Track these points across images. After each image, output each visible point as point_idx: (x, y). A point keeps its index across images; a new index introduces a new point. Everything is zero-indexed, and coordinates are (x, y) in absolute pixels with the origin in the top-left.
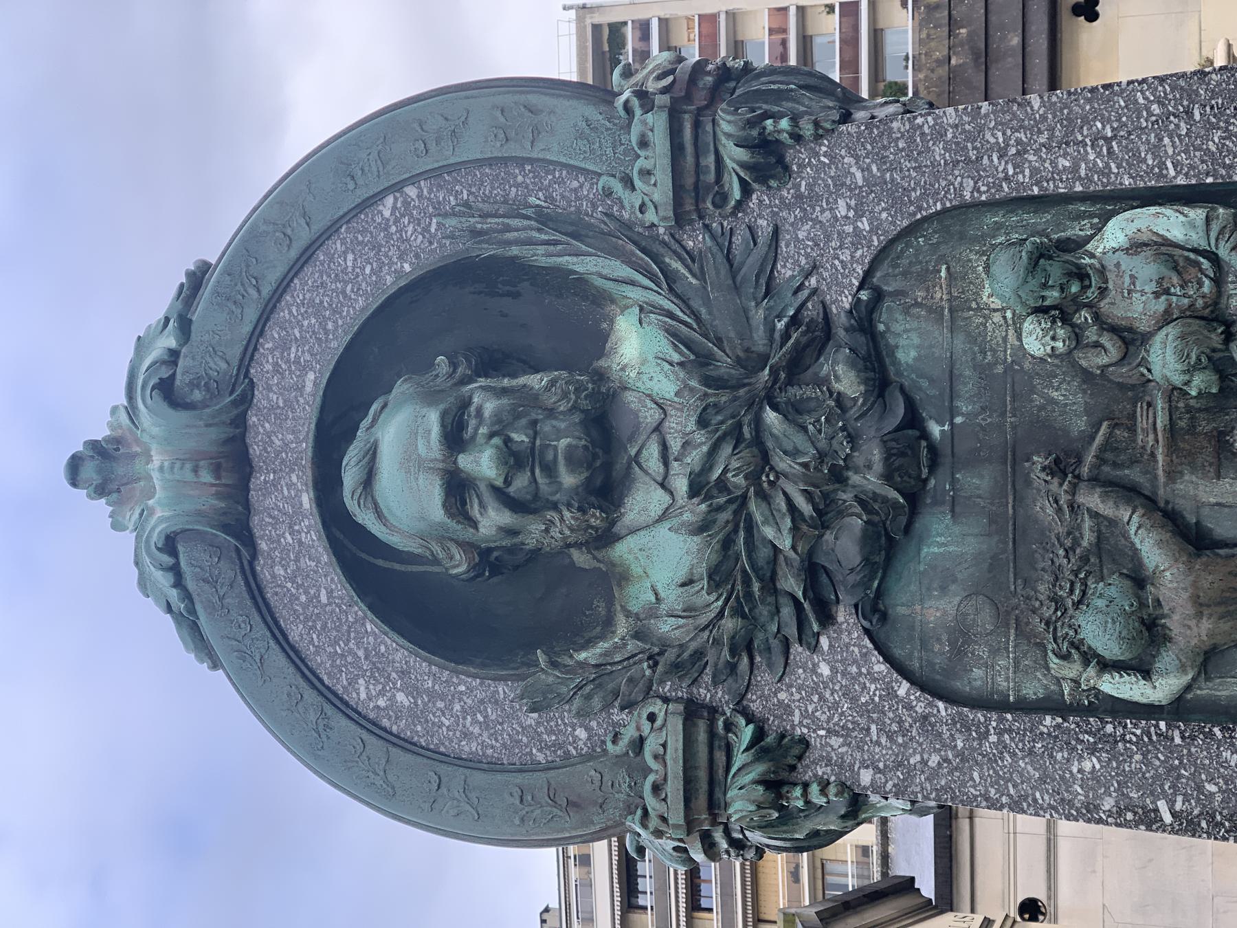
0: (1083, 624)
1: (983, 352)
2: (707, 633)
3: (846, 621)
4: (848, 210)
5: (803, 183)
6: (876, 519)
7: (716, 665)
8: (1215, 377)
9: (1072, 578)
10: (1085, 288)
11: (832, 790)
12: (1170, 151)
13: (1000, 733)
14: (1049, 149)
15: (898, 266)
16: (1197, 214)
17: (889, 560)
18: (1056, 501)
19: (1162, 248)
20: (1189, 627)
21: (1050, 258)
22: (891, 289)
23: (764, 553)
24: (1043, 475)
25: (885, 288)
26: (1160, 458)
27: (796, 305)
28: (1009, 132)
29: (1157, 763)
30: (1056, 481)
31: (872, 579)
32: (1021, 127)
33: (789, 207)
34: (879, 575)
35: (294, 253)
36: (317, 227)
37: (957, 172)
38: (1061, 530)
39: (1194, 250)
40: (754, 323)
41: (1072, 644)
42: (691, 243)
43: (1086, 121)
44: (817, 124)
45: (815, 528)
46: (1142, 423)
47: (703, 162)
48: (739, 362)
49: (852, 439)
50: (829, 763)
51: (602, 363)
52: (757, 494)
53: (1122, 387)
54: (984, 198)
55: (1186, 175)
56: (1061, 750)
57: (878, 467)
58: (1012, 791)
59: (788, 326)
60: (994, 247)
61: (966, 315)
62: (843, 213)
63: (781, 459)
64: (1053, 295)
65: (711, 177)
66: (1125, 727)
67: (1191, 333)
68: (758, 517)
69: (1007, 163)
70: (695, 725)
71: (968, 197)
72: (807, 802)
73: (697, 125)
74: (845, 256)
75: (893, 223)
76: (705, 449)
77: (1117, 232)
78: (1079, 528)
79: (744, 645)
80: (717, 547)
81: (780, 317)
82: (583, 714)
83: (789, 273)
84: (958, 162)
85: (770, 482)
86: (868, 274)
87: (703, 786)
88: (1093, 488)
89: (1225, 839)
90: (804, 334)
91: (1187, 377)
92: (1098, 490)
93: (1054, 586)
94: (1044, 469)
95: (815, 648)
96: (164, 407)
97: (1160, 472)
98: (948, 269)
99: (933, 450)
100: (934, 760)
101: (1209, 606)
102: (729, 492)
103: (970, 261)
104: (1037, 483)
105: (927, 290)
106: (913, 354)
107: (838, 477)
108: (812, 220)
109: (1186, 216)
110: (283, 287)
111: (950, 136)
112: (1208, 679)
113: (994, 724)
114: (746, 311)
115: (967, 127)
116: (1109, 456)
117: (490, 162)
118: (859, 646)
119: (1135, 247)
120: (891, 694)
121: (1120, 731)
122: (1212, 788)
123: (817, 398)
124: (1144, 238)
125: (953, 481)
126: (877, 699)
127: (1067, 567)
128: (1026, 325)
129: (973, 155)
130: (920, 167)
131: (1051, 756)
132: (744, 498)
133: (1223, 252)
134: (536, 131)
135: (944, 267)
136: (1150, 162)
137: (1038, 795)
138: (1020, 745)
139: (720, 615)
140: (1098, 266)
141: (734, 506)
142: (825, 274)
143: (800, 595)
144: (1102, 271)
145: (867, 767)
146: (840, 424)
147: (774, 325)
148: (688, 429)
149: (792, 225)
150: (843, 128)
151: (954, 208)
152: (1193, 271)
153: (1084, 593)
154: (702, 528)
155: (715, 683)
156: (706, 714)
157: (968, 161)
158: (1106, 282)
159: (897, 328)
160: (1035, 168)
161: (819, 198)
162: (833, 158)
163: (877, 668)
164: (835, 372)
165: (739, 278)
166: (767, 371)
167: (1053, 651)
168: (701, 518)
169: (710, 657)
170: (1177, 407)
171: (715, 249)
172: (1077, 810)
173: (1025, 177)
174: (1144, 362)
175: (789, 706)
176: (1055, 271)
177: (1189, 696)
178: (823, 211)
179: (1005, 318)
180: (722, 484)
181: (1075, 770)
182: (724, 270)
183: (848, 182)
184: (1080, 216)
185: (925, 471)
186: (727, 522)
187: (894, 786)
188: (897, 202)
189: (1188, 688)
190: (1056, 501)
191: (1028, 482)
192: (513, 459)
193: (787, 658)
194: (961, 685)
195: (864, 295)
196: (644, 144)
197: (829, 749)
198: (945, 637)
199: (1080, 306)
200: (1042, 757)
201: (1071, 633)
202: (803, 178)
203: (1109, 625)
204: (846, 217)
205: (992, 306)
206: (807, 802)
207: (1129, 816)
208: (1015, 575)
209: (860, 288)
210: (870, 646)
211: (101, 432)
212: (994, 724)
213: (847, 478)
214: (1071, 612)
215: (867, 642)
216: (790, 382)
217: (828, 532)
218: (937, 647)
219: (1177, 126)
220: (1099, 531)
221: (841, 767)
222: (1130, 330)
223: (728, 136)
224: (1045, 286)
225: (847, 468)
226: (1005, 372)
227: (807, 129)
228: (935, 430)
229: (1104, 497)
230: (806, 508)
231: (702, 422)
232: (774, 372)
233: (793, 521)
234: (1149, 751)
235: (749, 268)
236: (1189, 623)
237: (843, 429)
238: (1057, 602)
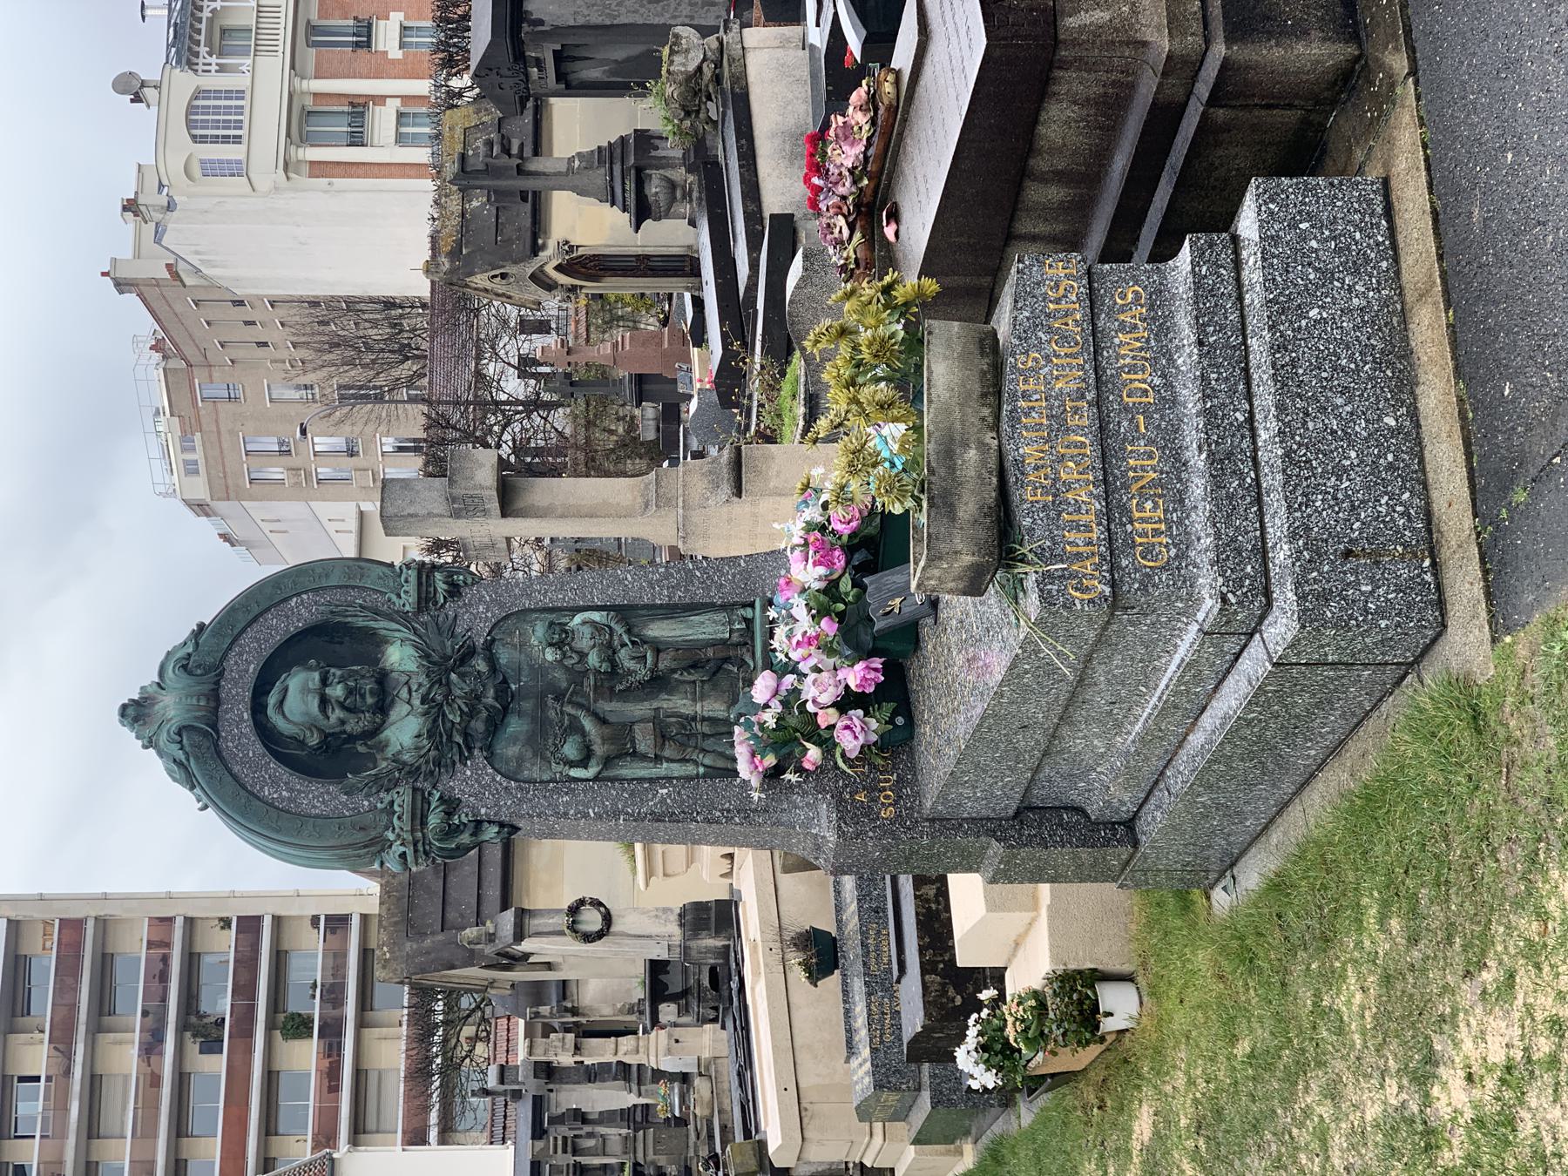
16: (605, 613)
17: (494, 733)
19: (593, 623)
35: (250, 618)
36: (261, 609)
51: (380, 665)
73: (428, 576)
77: (578, 619)
79: (438, 764)
82: (368, 796)
96: (185, 675)
107: (478, 698)
110: (244, 630)
117: (340, 587)
119: (584, 623)
120: (494, 780)
132: (442, 705)
134: (362, 576)
144: (573, 631)
154: (425, 714)
155: (425, 780)
173: (547, 601)
180: (433, 700)
188: (501, 606)
189: (599, 773)
192: (350, 692)
196: (406, 581)
211: (136, 697)
216: (460, 666)
228: (513, 687)
230: (466, 710)
238: (556, 745)
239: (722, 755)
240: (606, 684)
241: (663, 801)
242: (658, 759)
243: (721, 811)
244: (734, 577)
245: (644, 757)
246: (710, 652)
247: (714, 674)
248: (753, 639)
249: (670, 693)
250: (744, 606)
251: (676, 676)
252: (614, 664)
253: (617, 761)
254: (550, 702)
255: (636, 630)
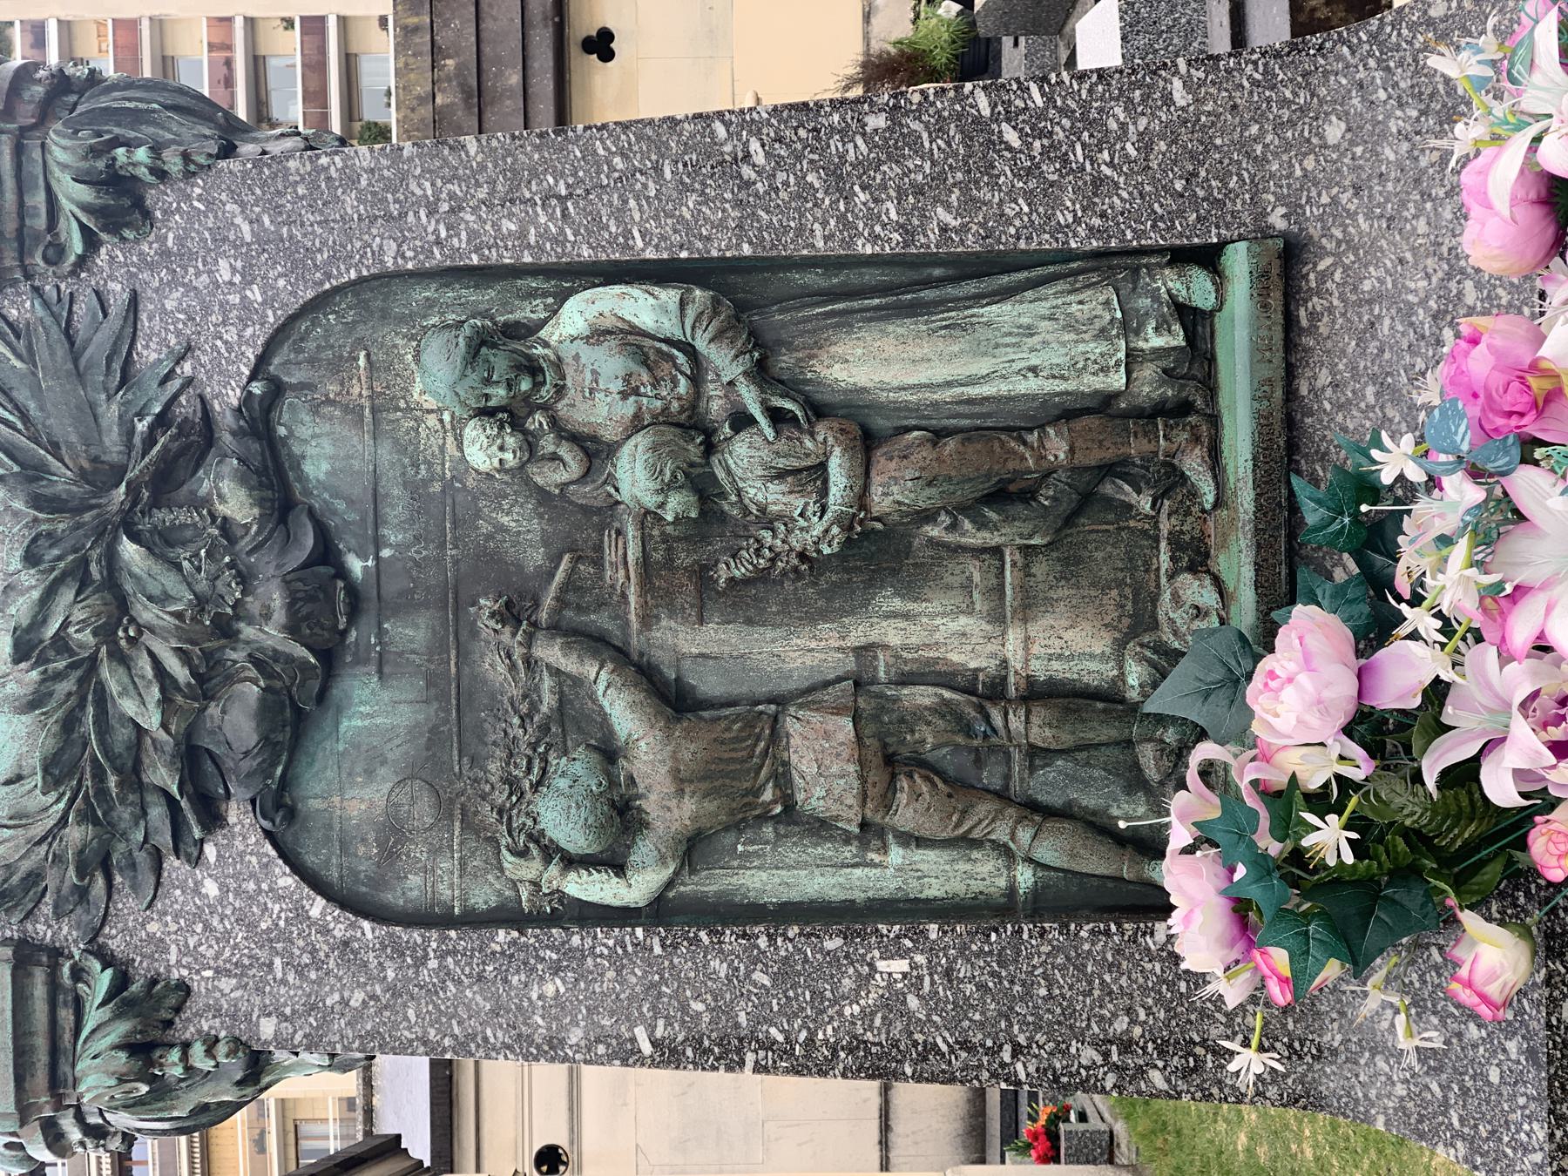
0: (542, 810)
1: (415, 465)
2: (44, 847)
3: (240, 822)
4: (233, 274)
5: (171, 236)
6: (278, 684)
7: (59, 891)
8: (693, 499)
9: (529, 752)
10: (537, 385)
11: (222, 1049)
12: (637, 217)
13: (441, 957)
14: (490, 207)
15: (299, 351)
16: (670, 296)
18: (509, 656)
19: (629, 337)
20: (669, 809)
21: (494, 346)
22: (293, 381)
23: (123, 734)
24: (492, 623)
25: (286, 379)
26: (632, 599)
27: (164, 399)
28: (439, 183)
29: (634, 980)
30: (508, 630)
31: (274, 765)
32: (454, 177)
33: (152, 267)
34: (284, 758)
37: (375, 231)
38: (516, 692)
39: (667, 341)
40: (104, 423)
41: (530, 837)
42: (15, 312)
43: (534, 174)
44: (186, 157)
45: (195, 699)
46: (610, 556)
47: (29, 201)
48: (83, 475)
49: (245, 579)
50: (218, 1013)
52: (110, 654)
53: (586, 510)
54: (410, 266)
55: (657, 247)
56: (518, 972)
57: (279, 616)
58: (457, 1030)
59: (152, 428)
60: (425, 329)
61: (392, 416)
62: (227, 277)
63: (146, 607)
64: (499, 394)
65: (41, 223)
66: (595, 937)
67: (664, 444)
68: (113, 687)
69: (438, 222)
70: (30, 975)
71: (390, 264)
72: (189, 1069)
74: (231, 335)
75: (294, 294)
76: (36, 594)
78: (537, 689)
79: (97, 861)
80: (55, 729)
81: (141, 415)
83: (154, 356)
84: (376, 218)
85: (130, 640)
86: (262, 360)
87: (42, 1058)
88: (553, 637)
89: (714, 1068)
90: (173, 438)
91: (661, 499)
92: (559, 641)
93: (508, 764)
94: (492, 615)
95: (197, 860)
97: (633, 617)
98: (368, 356)
99: (353, 591)
100: (357, 998)
101: (691, 781)
102: (72, 653)
103: (395, 346)
104: (486, 633)
105: (342, 384)
106: (325, 466)
107: (225, 629)
108: (183, 285)
109: (656, 298)
111: (364, 183)
112: (693, 872)
113: (434, 945)
114: (92, 406)
115: (386, 173)
116: (571, 597)
118: (258, 854)
119: (597, 335)
120: (301, 914)
121: (589, 942)
122: (698, 1006)
123: (195, 525)
124: (609, 323)
125: (381, 633)
126: (282, 923)
127: (524, 738)
128: (467, 430)
129: (394, 209)
130: (326, 221)
131: (505, 981)
132: (93, 661)
133: (701, 344)
135: (363, 354)
136: (613, 229)
137: (489, 1032)
138: (467, 970)
139: (63, 821)
140: (553, 357)
141: (79, 673)
142: (204, 359)
143: (174, 790)
144: (558, 364)
145: (269, 1015)
146: (227, 559)
147: (134, 427)
148: (12, 568)
149: (156, 291)
150: (222, 164)
151: (374, 277)
152: (666, 366)
153: (544, 771)
154: (33, 703)
155: (59, 914)
156: (45, 959)
157: (389, 217)
158: (563, 378)
159: (303, 432)
160: (474, 231)
161: (193, 256)
162: (209, 203)
163: (282, 882)
164: (218, 489)
165: (83, 362)
166: (123, 488)
167: (507, 847)
168: (32, 689)
169: (51, 880)
170: (651, 536)
171: (49, 320)
172: (538, 1047)
173: (461, 242)
174: (611, 479)
175: (162, 940)
176: (500, 364)
177: (671, 894)
178: (198, 274)
179: (441, 421)
180: (61, 642)
181: (534, 996)
182: (61, 350)
183: (232, 237)
184: (531, 295)
185: (342, 622)
186: (70, 694)
187: (305, 1036)
188: (297, 264)
189: (670, 884)
190: (509, 656)
191: (475, 633)
193: (159, 876)
194: (394, 898)
195: (257, 388)
197: (218, 995)
198: (371, 837)
199: (533, 409)
200: (494, 983)
201: (529, 822)
202: (170, 229)
203: (573, 811)
204: (231, 283)
205: (426, 406)
206: (189, 1069)
207: (601, 1049)
208: (460, 752)
209: (252, 378)
210: (273, 853)
212: (434, 945)
213: (239, 631)
214: (528, 796)
215: (268, 848)
216: (156, 503)
217: (213, 704)
218: (362, 850)
219: (645, 186)
220: (561, 693)
221: (234, 1017)
222: (594, 438)
223: (64, 167)
224: (488, 381)
225: (237, 617)
226: (443, 491)
227: (173, 163)
228: (356, 566)
229: (566, 648)
230: (180, 672)
231: (31, 558)
232: (133, 490)
233: (163, 690)
234: (623, 966)
235: (98, 347)
236: (668, 803)
237: (231, 566)
238: (512, 783)
239: (1099, 828)
240: (684, 559)
241: (892, 1003)
242: (870, 833)
243: (1102, 1044)
244: (1146, 146)
245: (821, 828)
246: (1057, 447)
247: (1069, 521)
248: (1210, 387)
249: (910, 590)
250: (1182, 257)
251: (934, 531)
252: (704, 488)
253: (728, 839)
254: (486, 624)
255: (785, 361)
